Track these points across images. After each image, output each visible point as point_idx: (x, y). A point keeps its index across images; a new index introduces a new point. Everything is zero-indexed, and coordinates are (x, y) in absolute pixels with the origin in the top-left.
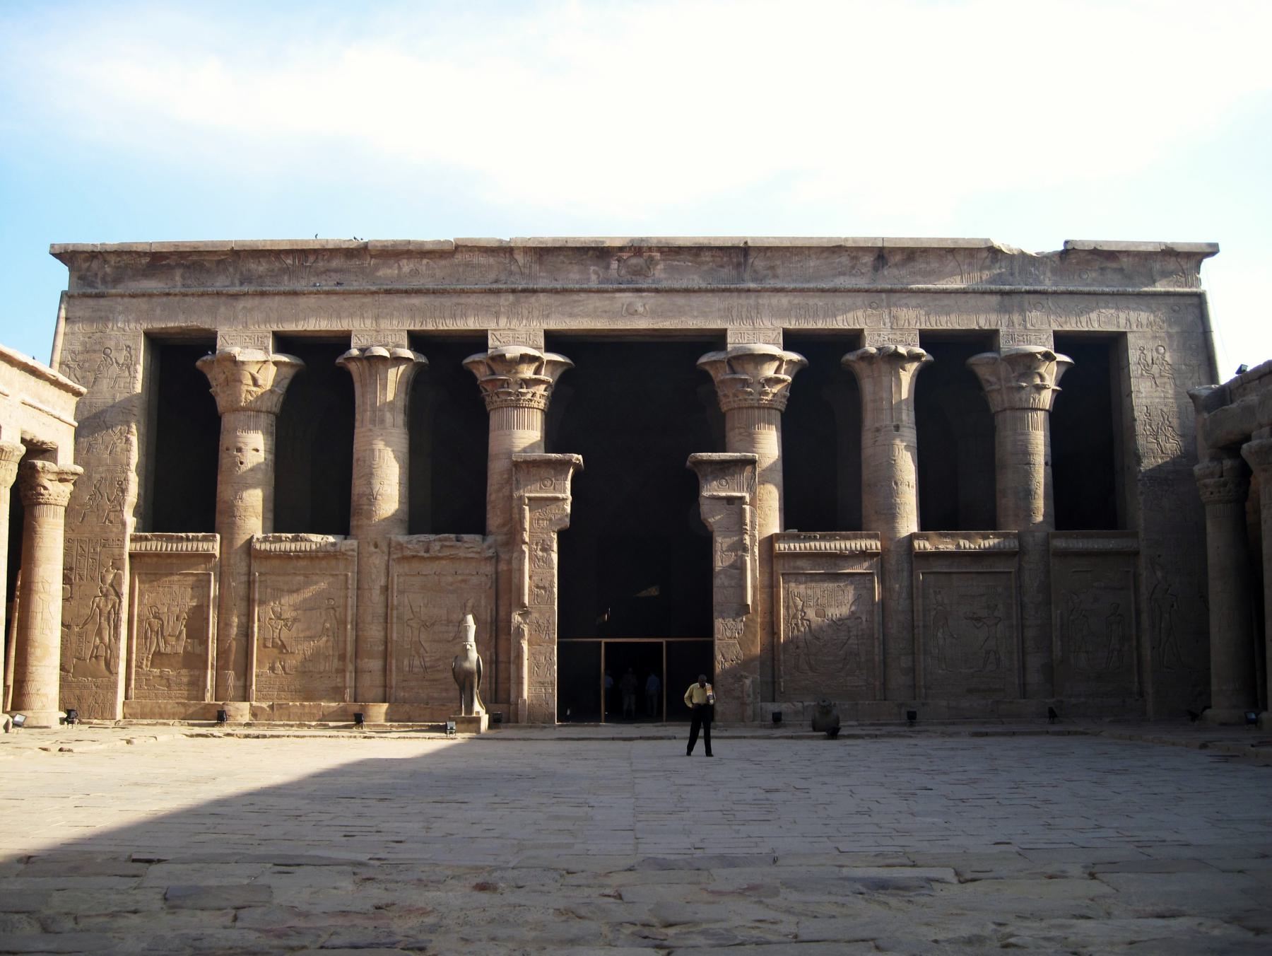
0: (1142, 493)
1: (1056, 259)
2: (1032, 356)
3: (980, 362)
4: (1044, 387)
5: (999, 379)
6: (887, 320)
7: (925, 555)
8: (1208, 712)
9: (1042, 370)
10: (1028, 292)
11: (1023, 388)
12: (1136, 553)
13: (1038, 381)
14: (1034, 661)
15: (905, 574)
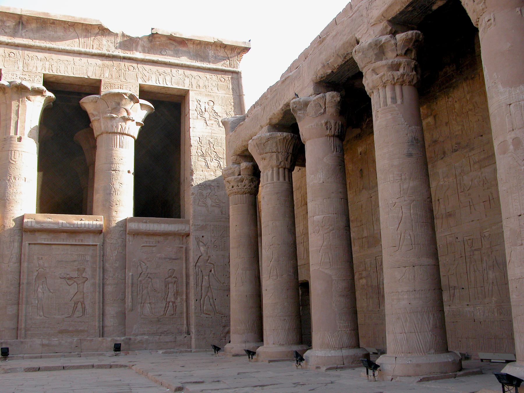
0: (193, 194)
1: (146, 40)
2: (120, 96)
3: (88, 103)
4: (129, 119)
5: (99, 113)
6: (21, 65)
7: (33, 231)
8: (228, 346)
9: (128, 107)
10: (124, 58)
11: (113, 117)
12: (188, 235)
13: (125, 114)
14: (111, 310)
15: (16, 245)
